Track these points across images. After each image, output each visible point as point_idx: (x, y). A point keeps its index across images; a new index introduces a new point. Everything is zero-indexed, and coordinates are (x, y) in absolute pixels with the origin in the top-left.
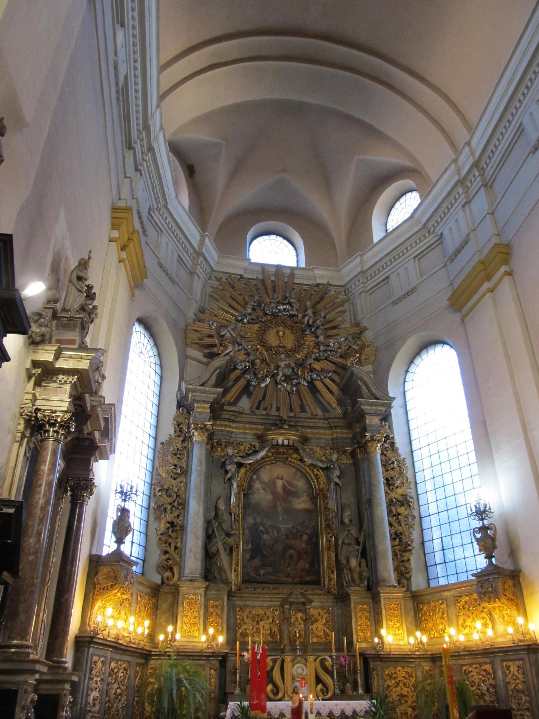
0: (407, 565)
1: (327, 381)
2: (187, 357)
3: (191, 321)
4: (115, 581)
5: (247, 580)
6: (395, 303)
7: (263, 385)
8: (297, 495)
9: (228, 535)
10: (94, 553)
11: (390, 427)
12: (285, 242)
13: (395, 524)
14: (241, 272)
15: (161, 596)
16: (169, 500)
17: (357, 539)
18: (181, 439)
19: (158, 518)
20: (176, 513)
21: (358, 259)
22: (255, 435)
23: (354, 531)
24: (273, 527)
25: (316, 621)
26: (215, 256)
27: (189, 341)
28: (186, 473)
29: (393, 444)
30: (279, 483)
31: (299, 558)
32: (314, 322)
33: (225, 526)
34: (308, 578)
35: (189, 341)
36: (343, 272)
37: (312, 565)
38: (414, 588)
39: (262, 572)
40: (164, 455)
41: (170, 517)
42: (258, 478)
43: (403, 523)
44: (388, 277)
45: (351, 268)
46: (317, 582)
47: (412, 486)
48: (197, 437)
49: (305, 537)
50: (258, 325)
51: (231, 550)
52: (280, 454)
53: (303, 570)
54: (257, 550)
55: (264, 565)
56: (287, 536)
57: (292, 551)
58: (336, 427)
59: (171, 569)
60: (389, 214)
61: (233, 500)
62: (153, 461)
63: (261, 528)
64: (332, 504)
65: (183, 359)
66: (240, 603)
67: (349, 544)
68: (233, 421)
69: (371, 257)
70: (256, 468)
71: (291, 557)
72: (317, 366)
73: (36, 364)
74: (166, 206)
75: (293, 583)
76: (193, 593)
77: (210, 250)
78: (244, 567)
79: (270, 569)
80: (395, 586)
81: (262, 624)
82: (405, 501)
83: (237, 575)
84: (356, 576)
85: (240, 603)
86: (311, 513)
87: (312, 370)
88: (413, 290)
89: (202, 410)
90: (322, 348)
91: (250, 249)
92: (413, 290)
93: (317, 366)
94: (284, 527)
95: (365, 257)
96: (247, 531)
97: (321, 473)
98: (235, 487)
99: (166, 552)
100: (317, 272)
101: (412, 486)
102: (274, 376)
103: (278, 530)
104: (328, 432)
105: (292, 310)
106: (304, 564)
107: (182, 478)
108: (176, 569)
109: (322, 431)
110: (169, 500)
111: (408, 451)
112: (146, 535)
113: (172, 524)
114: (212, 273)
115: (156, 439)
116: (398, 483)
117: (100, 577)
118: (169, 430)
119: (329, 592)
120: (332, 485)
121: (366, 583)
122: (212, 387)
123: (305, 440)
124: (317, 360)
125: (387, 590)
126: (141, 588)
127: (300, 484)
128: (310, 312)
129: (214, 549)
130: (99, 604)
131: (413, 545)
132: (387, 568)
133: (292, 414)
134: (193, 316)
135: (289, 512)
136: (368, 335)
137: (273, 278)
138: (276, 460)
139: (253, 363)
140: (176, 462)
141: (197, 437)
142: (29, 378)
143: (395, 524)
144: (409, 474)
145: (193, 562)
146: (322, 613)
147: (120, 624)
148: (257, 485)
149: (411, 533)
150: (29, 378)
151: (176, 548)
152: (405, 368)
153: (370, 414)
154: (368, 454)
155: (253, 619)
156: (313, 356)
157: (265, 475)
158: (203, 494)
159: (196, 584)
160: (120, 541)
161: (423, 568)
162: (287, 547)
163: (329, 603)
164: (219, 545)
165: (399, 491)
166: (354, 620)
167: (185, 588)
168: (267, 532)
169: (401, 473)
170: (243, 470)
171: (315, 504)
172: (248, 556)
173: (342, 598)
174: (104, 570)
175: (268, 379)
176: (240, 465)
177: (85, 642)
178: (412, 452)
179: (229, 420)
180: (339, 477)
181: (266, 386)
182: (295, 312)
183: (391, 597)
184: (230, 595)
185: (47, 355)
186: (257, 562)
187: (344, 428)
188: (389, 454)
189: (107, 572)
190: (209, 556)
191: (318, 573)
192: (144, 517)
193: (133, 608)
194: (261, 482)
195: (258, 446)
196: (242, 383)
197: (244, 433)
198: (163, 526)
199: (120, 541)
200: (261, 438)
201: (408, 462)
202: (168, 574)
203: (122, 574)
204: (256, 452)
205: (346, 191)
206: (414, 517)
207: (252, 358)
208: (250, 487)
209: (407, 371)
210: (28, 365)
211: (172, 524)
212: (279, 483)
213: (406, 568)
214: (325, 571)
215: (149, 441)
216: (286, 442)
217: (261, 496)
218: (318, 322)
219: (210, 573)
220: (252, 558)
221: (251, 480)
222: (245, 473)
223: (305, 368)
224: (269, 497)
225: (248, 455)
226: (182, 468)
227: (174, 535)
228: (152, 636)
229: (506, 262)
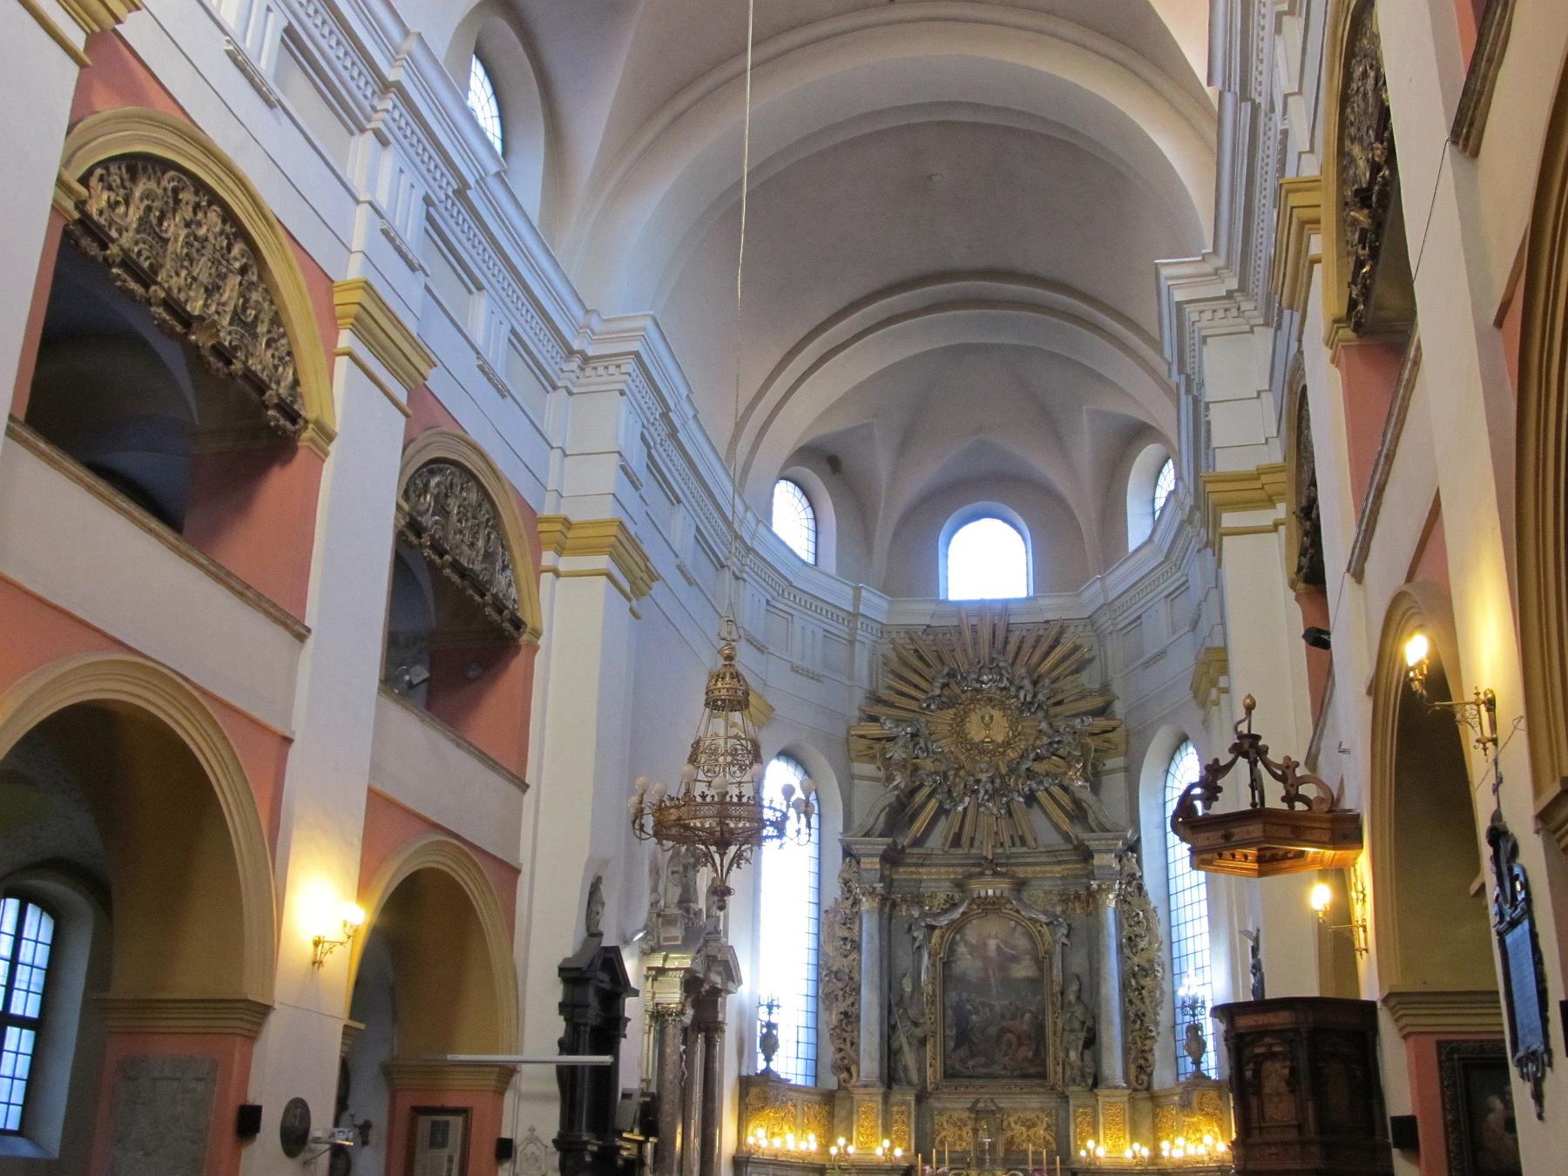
0: (1149, 1056)
1: (1056, 790)
2: (852, 777)
3: (854, 722)
4: (765, 1102)
5: (950, 1075)
6: (1146, 665)
7: (960, 808)
8: (1015, 959)
9: (916, 1024)
10: (744, 1073)
11: (1139, 861)
12: (1006, 527)
13: (1138, 1002)
14: (927, 621)
15: (830, 1101)
16: (840, 985)
17: (1083, 1023)
18: (850, 901)
19: (829, 1009)
20: (849, 1001)
21: (1098, 584)
22: (953, 881)
23: (1079, 1011)
24: (984, 1005)
25: (1034, 1125)
26: (885, 605)
27: (853, 754)
28: (857, 946)
29: (1140, 888)
30: (992, 944)
31: (1020, 1044)
32: (1035, 696)
33: (912, 1012)
34: (1032, 1071)
35: (853, 754)
36: (1087, 595)
37: (1037, 1052)
38: (1156, 1087)
39: (970, 1063)
40: (831, 925)
41: (842, 1007)
42: (962, 939)
43: (1147, 1001)
44: (1139, 617)
45: (1093, 594)
46: (1042, 1075)
47: (1165, 947)
48: (867, 904)
49: (1028, 1016)
50: (952, 711)
51: (923, 1042)
52: (990, 907)
53: (1025, 1059)
54: (963, 1036)
55: (973, 1056)
56: (1003, 1017)
57: (1010, 1035)
58: (1066, 862)
59: (848, 1070)
60: (1156, 485)
61: (923, 977)
62: (818, 935)
63: (969, 1007)
64: (1057, 973)
65: (847, 782)
66: (938, 1105)
67: (1072, 1031)
68: (922, 865)
69: (1121, 578)
70: (958, 927)
71: (1009, 1044)
72: (1039, 767)
73: (649, 969)
74: (791, 584)
75: (1012, 1077)
76: (869, 1104)
77: (875, 605)
78: (945, 1056)
79: (982, 1060)
80: (1117, 1087)
81: (965, 1130)
82: (1147, 971)
83: (935, 1072)
84: (1076, 1072)
85: (938, 1105)
86: (1036, 983)
87: (1030, 774)
88: (1161, 654)
89: (872, 864)
90: (1045, 740)
91: (950, 552)
92: (1161, 654)
93: (1039, 767)
94: (999, 1004)
95: (1111, 580)
96: (950, 1012)
97: (1045, 929)
98: (926, 957)
99: (841, 1050)
100: (1043, 602)
101: (1165, 947)
102: (975, 792)
103: (992, 1008)
104: (1057, 868)
105: (1001, 680)
106: (1026, 1052)
107: (854, 955)
108: (853, 1069)
109: (1048, 868)
110: (840, 985)
111: (1163, 895)
112: (817, 1029)
113: (846, 1014)
114: (884, 629)
115: (819, 904)
116: (1142, 944)
117: (751, 1098)
118: (834, 891)
119: (1053, 1088)
120: (1058, 948)
121: (1090, 1081)
122: (880, 836)
123: (1020, 885)
124: (1038, 758)
125: (1106, 1092)
126: (807, 1097)
127: (1022, 943)
128: (1027, 683)
129: (895, 1045)
130: (751, 1127)
131: (1161, 1029)
132: (1114, 1064)
133: (1000, 850)
134: (857, 713)
135: (1008, 983)
136: (1119, 708)
137: (974, 621)
138: (986, 912)
139: (945, 777)
140: (846, 934)
141: (867, 904)
142: (647, 978)
143: (1138, 1002)
144: (1161, 931)
145: (869, 1063)
146: (1042, 1116)
147: (777, 1143)
148: (962, 949)
149: (1156, 1014)
150: (647, 978)
151: (852, 1044)
152: (1164, 767)
153: (1100, 851)
154: (1097, 908)
155: (954, 1124)
156: (1032, 756)
157: (971, 934)
158: (877, 979)
159: (871, 1090)
160: (768, 1059)
161: (1172, 1060)
162: (1003, 1031)
163: (1052, 1102)
164: (902, 1039)
165: (1145, 955)
166: (1072, 1127)
167: (858, 1094)
168: (977, 1012)
169: (1148, 929)
170: (937, 932)
171: (1041, 970)
172: (952, 1044)
173: (1065, 1098)
174: (754, 1091)
175: (967, 799)
176: (932, 928)
177: (741, 1162)
178: (1169, 896)
179: (916, 865)
180: (1067, 936)
181: (965, 809)
182: (1005, 683)
183: (1113, 1102)
184: (921, 1098)
185: (657, 962)
186: (963, 1052)
187: (1076, 862)
188: (1135, 900)
189: (760, 1091)
190: (890, 1054)
191: (1043, 1064)
192: (812, 1008)
193: (799, 1121)
194: (967, 944)
195: (957, 896)
196: (933, 805)
197: (936, 881)
198: (834, 1018)
199: (768, 1059)
200: (960, 885)
201: (1161, 913)
202: (844, 1075)
203: (772, 1094)
204: (955, 906)
205: (1086, 449)
206: (1163, 992)
207: (943, 768)
208: (951, 951)
209: (1167, 771)
210: (645, 972)
211: (846, 1014)
212: (992, 944)
213: (1146, 1060)
214: (1050, 1062)
215: (812, 911)
216: (990, 892)
217: (966, 963)
218: (1041, 697)
219: (891, 1077)
220: (958, 1046)
221: (953, 943)
222: (942, 937)
223: (1019, 776)
224: (979, 964)
225: (945, 911)
226: (853, 941)
227: (849, 1028)
228: (825, 1147)
229: (1224, 669)
